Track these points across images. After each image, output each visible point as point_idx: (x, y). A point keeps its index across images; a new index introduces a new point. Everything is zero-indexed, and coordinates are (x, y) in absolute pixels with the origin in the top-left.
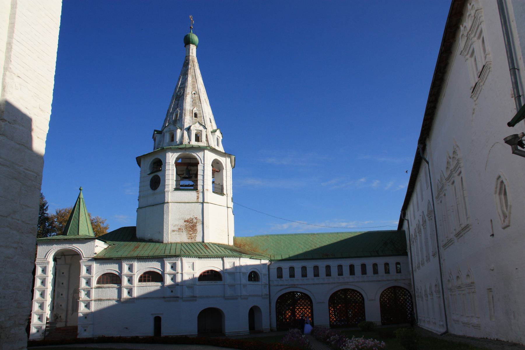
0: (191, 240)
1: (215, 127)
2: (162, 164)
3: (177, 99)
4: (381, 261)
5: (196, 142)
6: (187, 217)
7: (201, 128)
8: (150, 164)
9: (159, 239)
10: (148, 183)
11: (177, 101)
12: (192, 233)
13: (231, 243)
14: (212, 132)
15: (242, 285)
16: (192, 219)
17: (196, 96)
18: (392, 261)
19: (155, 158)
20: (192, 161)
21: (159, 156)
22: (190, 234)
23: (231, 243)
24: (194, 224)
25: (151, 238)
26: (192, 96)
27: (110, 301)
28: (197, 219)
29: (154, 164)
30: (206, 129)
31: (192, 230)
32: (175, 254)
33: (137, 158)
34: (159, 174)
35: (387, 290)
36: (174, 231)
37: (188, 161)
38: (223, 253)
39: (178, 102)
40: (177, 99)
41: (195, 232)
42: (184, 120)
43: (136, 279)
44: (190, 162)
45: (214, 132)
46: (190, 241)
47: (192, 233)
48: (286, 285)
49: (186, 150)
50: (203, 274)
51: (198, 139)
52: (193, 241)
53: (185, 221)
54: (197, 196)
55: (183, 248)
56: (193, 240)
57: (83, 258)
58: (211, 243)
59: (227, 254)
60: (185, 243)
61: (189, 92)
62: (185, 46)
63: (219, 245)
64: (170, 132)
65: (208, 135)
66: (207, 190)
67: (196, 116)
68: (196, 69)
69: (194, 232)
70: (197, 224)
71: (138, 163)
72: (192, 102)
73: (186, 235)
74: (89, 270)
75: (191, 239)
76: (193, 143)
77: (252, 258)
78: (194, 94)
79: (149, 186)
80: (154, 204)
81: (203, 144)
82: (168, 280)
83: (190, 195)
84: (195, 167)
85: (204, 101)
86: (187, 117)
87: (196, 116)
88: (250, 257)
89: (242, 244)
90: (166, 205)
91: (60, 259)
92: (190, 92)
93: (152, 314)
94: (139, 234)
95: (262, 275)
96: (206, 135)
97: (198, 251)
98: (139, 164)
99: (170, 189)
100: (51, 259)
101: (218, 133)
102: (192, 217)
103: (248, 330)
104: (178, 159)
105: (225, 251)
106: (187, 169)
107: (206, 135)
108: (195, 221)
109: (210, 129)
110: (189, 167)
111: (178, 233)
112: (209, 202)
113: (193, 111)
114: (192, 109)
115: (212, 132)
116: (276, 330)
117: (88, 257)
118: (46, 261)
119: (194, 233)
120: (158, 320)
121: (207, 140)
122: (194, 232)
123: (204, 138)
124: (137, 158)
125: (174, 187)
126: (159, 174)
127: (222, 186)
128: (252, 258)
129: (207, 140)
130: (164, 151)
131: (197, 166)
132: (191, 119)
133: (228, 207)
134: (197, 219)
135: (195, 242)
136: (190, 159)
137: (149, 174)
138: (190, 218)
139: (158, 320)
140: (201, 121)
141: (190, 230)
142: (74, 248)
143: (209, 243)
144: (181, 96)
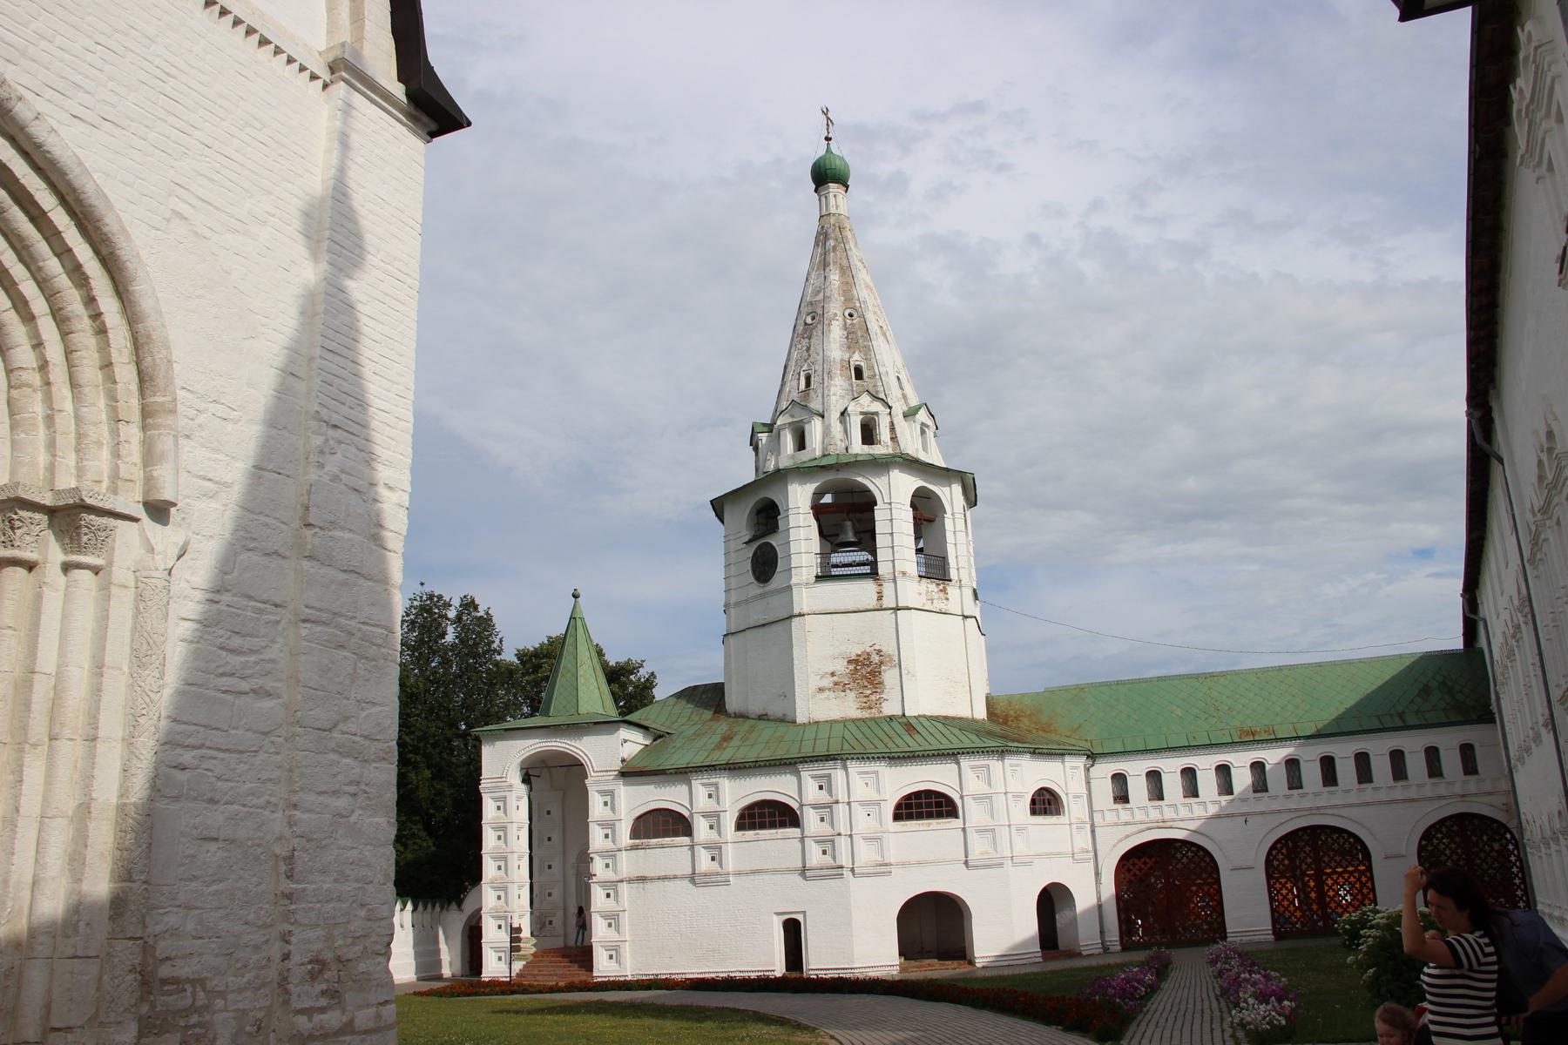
0: (869, 711)
3: (805, 336)
4: (1414, 744)
5: (866, 447)
6: (854, 650)
7: (877, 407)
8: (748, 516)
9: (784, 715)
11: (807, 340)
12: (869, 692)
14: (906, 416)
15: (1013, 828)
16: (868, 654)
17: (855, 322)
18: (1449, 741)
19: (762, 496)
23: (981, 713)
24: (875, 668)
25: (764, 712)
26: (846, 324)
27: (667, 883)
28: (882, 653)
29: (757, 514)
30: (890, 408)
31: (871, 683)
32: (826, 753)
33: (712, 502)
34: (774, 541)
35: (1438, 826)
36: (821, 690)
38: (956, 744)
39: (810, 343)
40: (805, 336)
41: (879, 691)
42: (829, 390)
43: (730, 821)
46: (865, 714)
47: (869, 692)
48: (1141, 823)
49: (838, 470)
51: (869, 435)
52: (874, 713)
53: (850, 662)
55: (848, 736)
57: (593, 774)
58: (924, 716)
59: (967, 743)
60: (854, 721)
61: (834, 311)
62: (816, 191)
63: (946, 721)
65: (895, 422)
66: (904, 573)
67: (859, 373)
68: (850, 249)
71: (717, 515)
72: (847, 338)
74: (611, 804)
76: (858, 447)
77: (1037, 751)
78: (851, 315)
80: (765, 622)
81: (882, 449)
82: (812, 823)
83: (863, 591)
85: (879, 332)
86: (836, 379)
87: (859, 373)
88: (1032, 750)
89: (1012, 713)
91: (538, 776)
92: (839, 313)
93: (778, 914)
94: (733, 702)
95: (1070, 796)
96: (892, 424)
97: (887, 740)
98: (720, 516)
100: (515, 778)
102: (868, 650)
103: (1039, 950)
104: (818, 494)
105: (963, 738)
107: (892, 424)
108: (875, 658)
109: (899, 408)
112: (910, 606)
113: (852, 363)
114: (846, 357)
116: (1119, 948)
118: (505, 784)
120: (793, 930)
121: (894, 439)
123: (884, 433)
124: (711, 502)
125: (815, 570)
126: (774, 541)
127: (944, 559)
128: (1037, 751)
129: (894, 439)
130: (780, 477)
131: (873, 511)
132: (846, 385)
134: (882, 653)
135: (881, 715)
136: (852, 492)
137: (746, 543)
139: (793, 930)
140: (875, 386)
141: (866, 684)
142: (569, 747)
143: (919, 716)
144: (816, 326)
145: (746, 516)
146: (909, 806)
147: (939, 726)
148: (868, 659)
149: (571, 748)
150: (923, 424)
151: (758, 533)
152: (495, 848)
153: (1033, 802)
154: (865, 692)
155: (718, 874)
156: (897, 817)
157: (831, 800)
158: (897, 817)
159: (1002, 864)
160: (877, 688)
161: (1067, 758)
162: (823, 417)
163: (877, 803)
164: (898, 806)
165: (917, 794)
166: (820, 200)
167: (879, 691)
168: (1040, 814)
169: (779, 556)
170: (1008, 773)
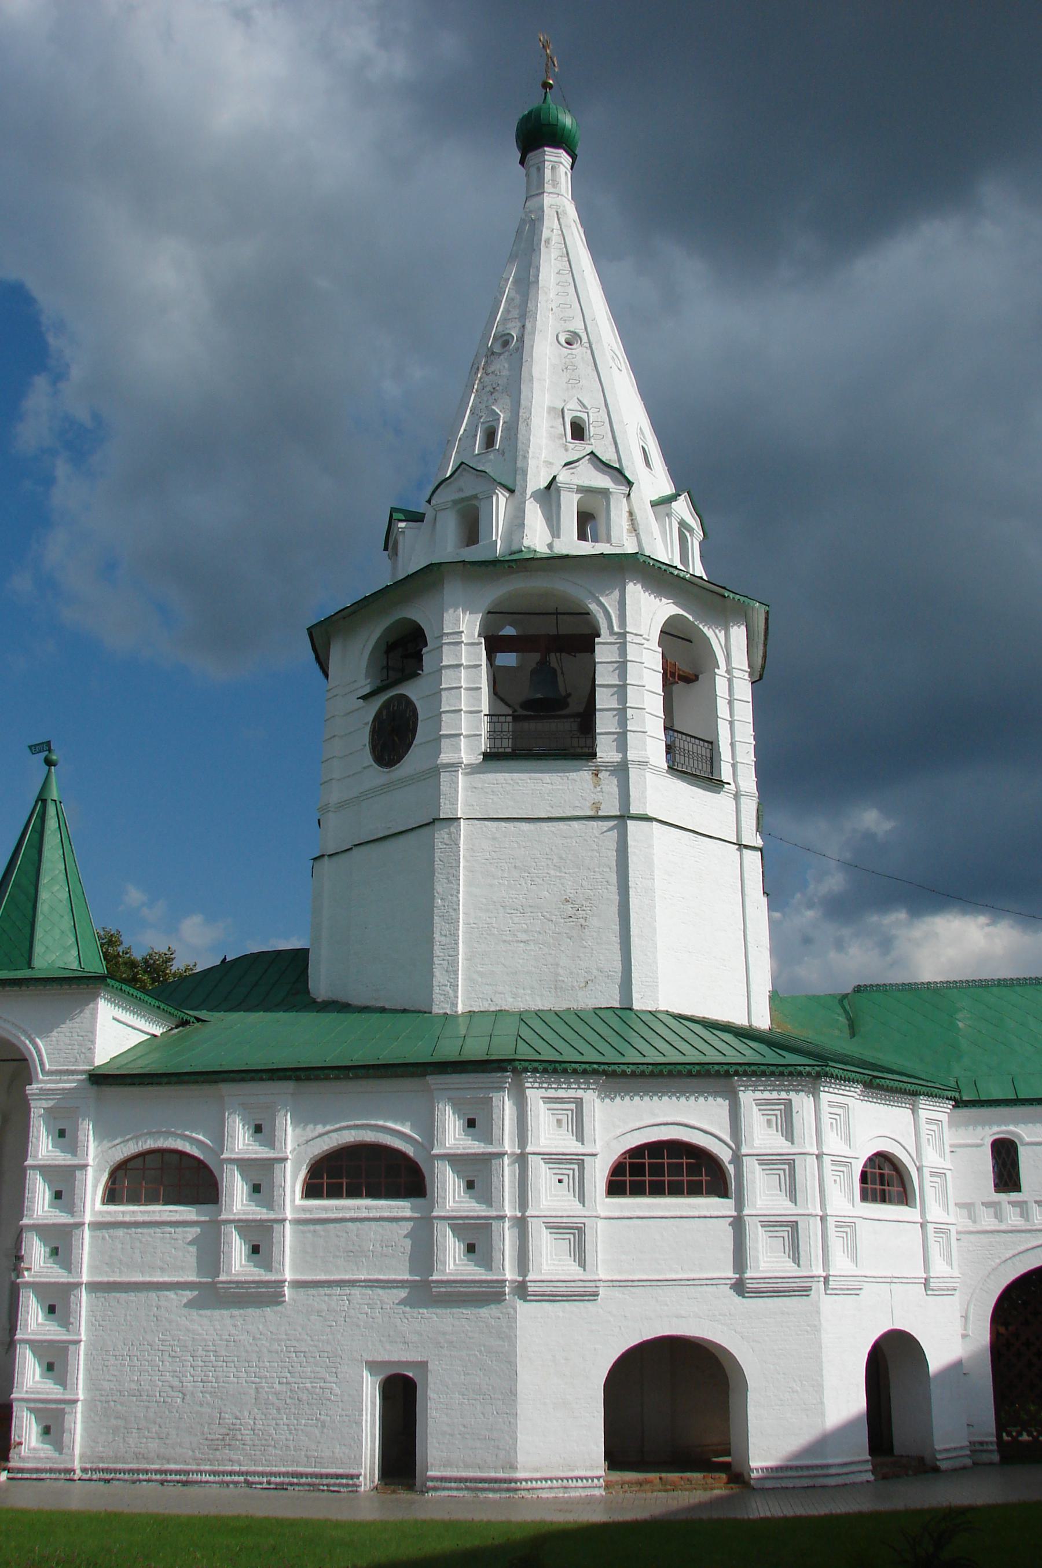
1: (667, 488)
2: (426, 645)
8: (372, 652)
10: (364, 737)
13: (762, 1021)
20: (568, 627)
21: (417, 613)
34: (412, 691)
37: (545, 627)
38: (733, 1057)
44: (553, 632)
45: (662, 503)
50: (628, 1160)
51: (587, 522)
55: (526, 1033)
58: (667, 1013)
60: (538, 1014)
62: (522, 162)
64: (459, 506)
65: (636, 511)
76: (570, 544)
79: (367, 750)
84: (586, 656)
87: (578, 431)
90: (441, 835)
95: (926, 1171)
99: (463, 755)
101: (682, 507)
106: (543, 663)
107: (631, 514)
110: (553, 659)
112: (651, 814)
115: (654, 504)
116: (996, 1458)
124: (310, 631)
125: (483, 745)
126: (412, 691)
127: (712, 744)
131: (592, 650)
133: (741, 846)
136: (557, 614)
137: (364, 698)
145: (364, 663)
146: (637, 1169)
147: (698, 1028)
150: (682, 524)
151: (384, 683)
153: (864, 1177)
156: (615, 1188)
158: (615, 1188)
159: (808, 1289)
161: (923, 1102)
162: (512, 491)
163: (579, 1161)
164: (617, 1170)
165: (655, 1148)
166: (527, 175)
168: (874, 1200)
169: (420, 718)
170: (826, 1119)
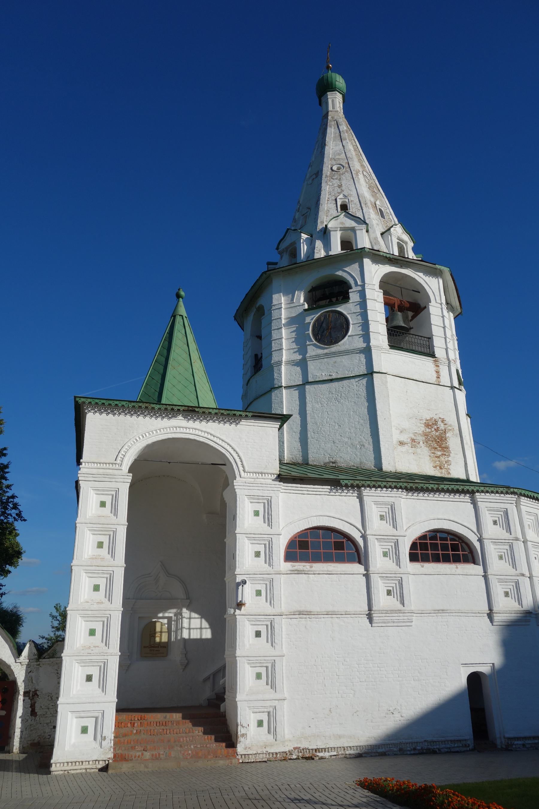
0: (440, 471)
22: (436, 457)
36: (401, 443)
41: (447, 454)
47: (439, 453)
54: (436, 372)
56: (443, 471)
69: (445, 453)
70: (447, 435)
73: (429, 458)
75: (441, 468)
102: (436, 417)
111: (411, 450)
117: (260, 471)
119: (445, 455)
122: (445, 453)
134: (446, 422)
138: (431, 419)
142: (212, 438)
148: (436, 425)
149: (215, 439)
152: (93, 558)
154: (436, 452)
155: (399, 611)
157: (511, 537)
160: (445, 451)
167: (447, 454)
